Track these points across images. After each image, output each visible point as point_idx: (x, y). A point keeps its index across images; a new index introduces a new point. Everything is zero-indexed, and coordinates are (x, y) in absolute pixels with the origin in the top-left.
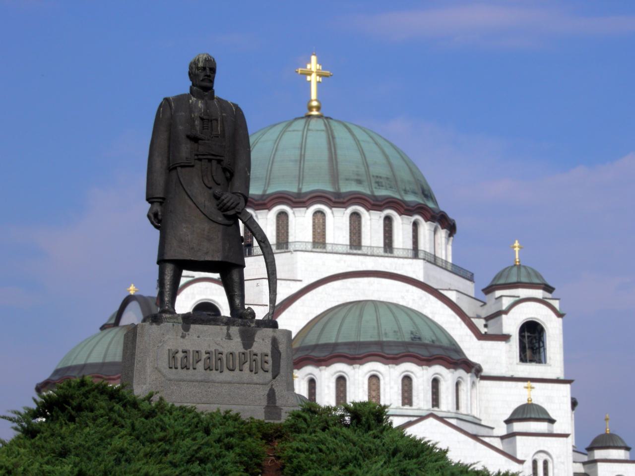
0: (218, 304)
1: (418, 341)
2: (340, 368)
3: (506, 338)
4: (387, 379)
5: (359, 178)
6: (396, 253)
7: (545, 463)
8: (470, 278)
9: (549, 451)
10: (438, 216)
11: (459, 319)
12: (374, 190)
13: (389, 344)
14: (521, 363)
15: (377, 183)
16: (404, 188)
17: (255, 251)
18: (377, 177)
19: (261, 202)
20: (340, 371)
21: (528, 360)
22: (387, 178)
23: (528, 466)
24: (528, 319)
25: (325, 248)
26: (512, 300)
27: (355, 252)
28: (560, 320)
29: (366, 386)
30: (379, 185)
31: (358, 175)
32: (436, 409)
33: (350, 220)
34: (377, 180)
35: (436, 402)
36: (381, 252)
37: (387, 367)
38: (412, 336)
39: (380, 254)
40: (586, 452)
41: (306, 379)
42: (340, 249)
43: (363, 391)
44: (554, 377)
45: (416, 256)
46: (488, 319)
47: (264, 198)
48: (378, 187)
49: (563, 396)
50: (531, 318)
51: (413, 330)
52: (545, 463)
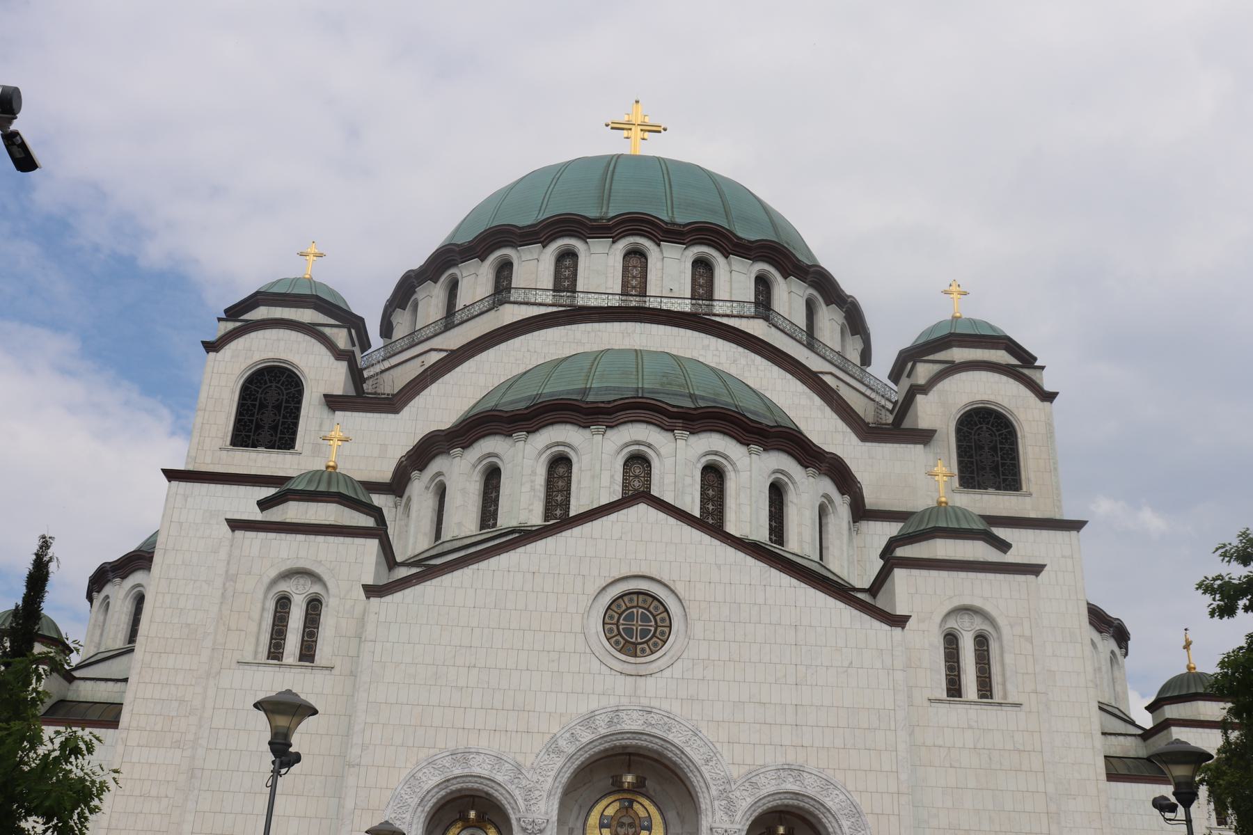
0: (297, 367)
1: (676, 389)
3: (924, 437)
4: (586, 459)
7: (982, 641)
9: (988, 608)
11: (818, 401)
12: (675, 216)
20: (490, 455)
24: (973, 403)
26: (937, 368)
37: (586, 433)
40: (1146, 721)
43: (533, 489)
49: (1063, 557)
50: (982, 402)
52: (982, 641)
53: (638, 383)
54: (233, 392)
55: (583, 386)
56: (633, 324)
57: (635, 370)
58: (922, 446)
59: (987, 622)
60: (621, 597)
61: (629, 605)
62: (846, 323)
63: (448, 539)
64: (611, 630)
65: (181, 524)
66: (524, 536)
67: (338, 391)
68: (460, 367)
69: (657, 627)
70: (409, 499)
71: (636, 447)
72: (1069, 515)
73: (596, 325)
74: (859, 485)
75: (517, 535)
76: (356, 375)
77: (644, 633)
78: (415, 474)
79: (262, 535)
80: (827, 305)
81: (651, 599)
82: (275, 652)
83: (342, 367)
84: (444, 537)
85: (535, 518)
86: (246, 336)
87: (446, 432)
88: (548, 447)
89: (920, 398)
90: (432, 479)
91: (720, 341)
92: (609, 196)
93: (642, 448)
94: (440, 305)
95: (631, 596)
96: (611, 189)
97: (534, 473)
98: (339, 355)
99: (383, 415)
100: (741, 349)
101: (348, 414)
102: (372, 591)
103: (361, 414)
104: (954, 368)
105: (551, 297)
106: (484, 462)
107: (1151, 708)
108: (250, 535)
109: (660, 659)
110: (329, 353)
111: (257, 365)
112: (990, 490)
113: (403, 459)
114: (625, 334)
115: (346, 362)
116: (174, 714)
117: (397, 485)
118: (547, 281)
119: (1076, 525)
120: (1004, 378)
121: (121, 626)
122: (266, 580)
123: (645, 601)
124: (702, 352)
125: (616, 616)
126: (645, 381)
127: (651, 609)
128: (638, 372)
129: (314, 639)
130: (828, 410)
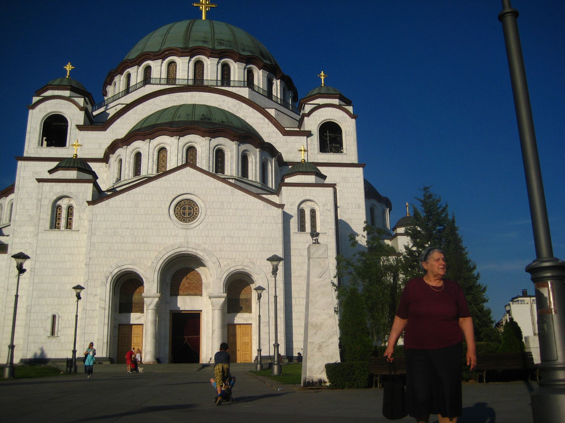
0: (65, 114)
2: (139, 145)
5: (206, 40)
9: (315, 200)
11: (266, 120)
12: (215, 46)
14: (321, 153)
15: (218, 43)
16: (243, 48)
18: (220, 40)
20: (137, 148)
21: (329, 152)
22: (229, 41)
23: (292, 211)
26: (314, 106)
28: (354, 120)
29: (156, 157)
30: (221, 44)
31: (205, 38)
32: (220, 175)
34: (220, 41)
38: (203, 117)
43: (153, 161)
44: (349, 162)
48: (219, 45)
49: (357, 177)
51: (205, 113)
52: (313, 212)
53: (192, 119)
54: (41, 125)
55: (172, 121)
56: (196, 92)
57: (191, 113)
59: (316, 205)
60: (181, 201)
61: (184, 204)
62: (286, 86)
63: (123, 180)
64: (177, 213)
65: (24, 177)
66: (150, 179)
67: (82, 123)
68: (129, 112)
70: (110, 164)
73: (181, 94)
74: (279, 153)
75: (147, 178)
76: (88, 115)
77: (189, 214)
78: (111, 155)
79: (49, 184)
81: (192, 202)
83: (82, 113)
84: (122, 179)
85: (153, 172)
86: (44, 103)
87: (121, 140)
89: (306, 118)
90: (117, 157)
91: (230, 98)
92: (189, 38)
93: (194, 144)
94: (124, 84)
95: (184, 201)
96: (190, 36)
97: (153, 155)
98: (81, 109)
99: (100, 132)
100: (237, 101)
101: (86, 132)
102: (89, 203)
103: (91, 132)
104: (319, 107)
105: (166, 81)
106: (135, 151)
108: (45, 184)
109: (195, 223)
110: (77, 108)
111: (49, 114)
112: (331, 153)
113: (106, 150)
114: (192, 97)
115: (84, 112)
116: (28, 248)
117: (105, 159)
118: (164, 75)
120: (338, 110)
121: (8, 215)
122: (52, 201)
123: (189, 202)
124: (222, 103)
125: (179, 208)
126: (195, 118)
127: (192, 205)
128: (193, 114)
129: (72, 221)
130: (270, 124)
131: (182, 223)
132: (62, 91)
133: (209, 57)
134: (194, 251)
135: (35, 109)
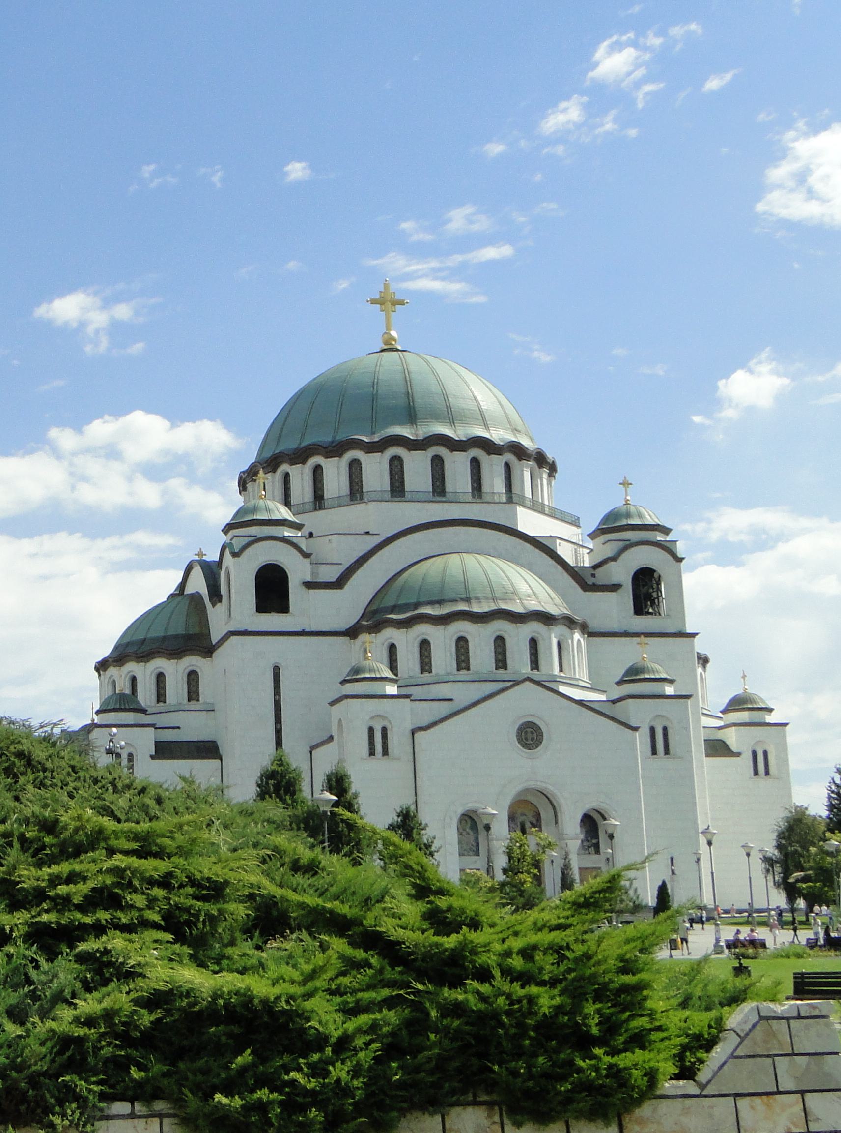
2: (423, 630)
3: (614, 587)
6: (487, 498)
8: (575, 523)
10: (534, 454)
13: (477, 599)
17: (326, 504)
19: (330, 448)
23: (645, 731)
25: (404, 496)
26: (621, 544)
27: (438, 499)
32: (535, 672)
33: (432, 464)
35: (535, 664)
36: (469, 497)
39: (467, 501)
41: (386, 645)
42: (421, 497)
43: (451, 654)
45: (510, 500)
46: (596, 567)
47: (334, 444)
52: (665, 729)
58: (614, 593)
69: (537, 736)
71: (498, 634)
72: (688, 631)
77: (532, 739)
79: (359, 700)
80: (540, 468)
82: (372, 753)
88: (456, 633)
99: (335, 590)
104: (629, 545)
107: (723, 712)
119: (693, 635)
130: (565, 574)
131: (525, 750)
132: (273, 527)
133: (452, 450)
134: (544, 785)
135: (241, 556)
